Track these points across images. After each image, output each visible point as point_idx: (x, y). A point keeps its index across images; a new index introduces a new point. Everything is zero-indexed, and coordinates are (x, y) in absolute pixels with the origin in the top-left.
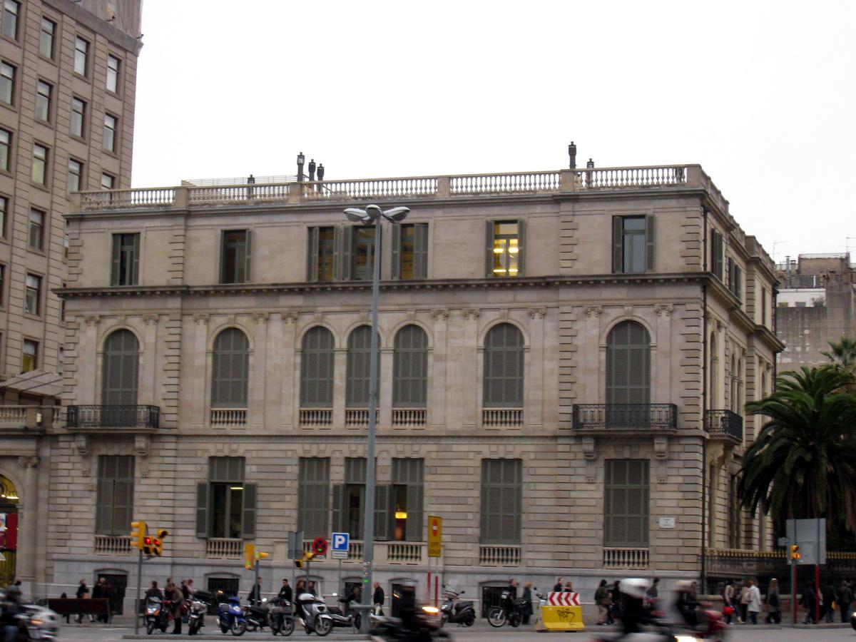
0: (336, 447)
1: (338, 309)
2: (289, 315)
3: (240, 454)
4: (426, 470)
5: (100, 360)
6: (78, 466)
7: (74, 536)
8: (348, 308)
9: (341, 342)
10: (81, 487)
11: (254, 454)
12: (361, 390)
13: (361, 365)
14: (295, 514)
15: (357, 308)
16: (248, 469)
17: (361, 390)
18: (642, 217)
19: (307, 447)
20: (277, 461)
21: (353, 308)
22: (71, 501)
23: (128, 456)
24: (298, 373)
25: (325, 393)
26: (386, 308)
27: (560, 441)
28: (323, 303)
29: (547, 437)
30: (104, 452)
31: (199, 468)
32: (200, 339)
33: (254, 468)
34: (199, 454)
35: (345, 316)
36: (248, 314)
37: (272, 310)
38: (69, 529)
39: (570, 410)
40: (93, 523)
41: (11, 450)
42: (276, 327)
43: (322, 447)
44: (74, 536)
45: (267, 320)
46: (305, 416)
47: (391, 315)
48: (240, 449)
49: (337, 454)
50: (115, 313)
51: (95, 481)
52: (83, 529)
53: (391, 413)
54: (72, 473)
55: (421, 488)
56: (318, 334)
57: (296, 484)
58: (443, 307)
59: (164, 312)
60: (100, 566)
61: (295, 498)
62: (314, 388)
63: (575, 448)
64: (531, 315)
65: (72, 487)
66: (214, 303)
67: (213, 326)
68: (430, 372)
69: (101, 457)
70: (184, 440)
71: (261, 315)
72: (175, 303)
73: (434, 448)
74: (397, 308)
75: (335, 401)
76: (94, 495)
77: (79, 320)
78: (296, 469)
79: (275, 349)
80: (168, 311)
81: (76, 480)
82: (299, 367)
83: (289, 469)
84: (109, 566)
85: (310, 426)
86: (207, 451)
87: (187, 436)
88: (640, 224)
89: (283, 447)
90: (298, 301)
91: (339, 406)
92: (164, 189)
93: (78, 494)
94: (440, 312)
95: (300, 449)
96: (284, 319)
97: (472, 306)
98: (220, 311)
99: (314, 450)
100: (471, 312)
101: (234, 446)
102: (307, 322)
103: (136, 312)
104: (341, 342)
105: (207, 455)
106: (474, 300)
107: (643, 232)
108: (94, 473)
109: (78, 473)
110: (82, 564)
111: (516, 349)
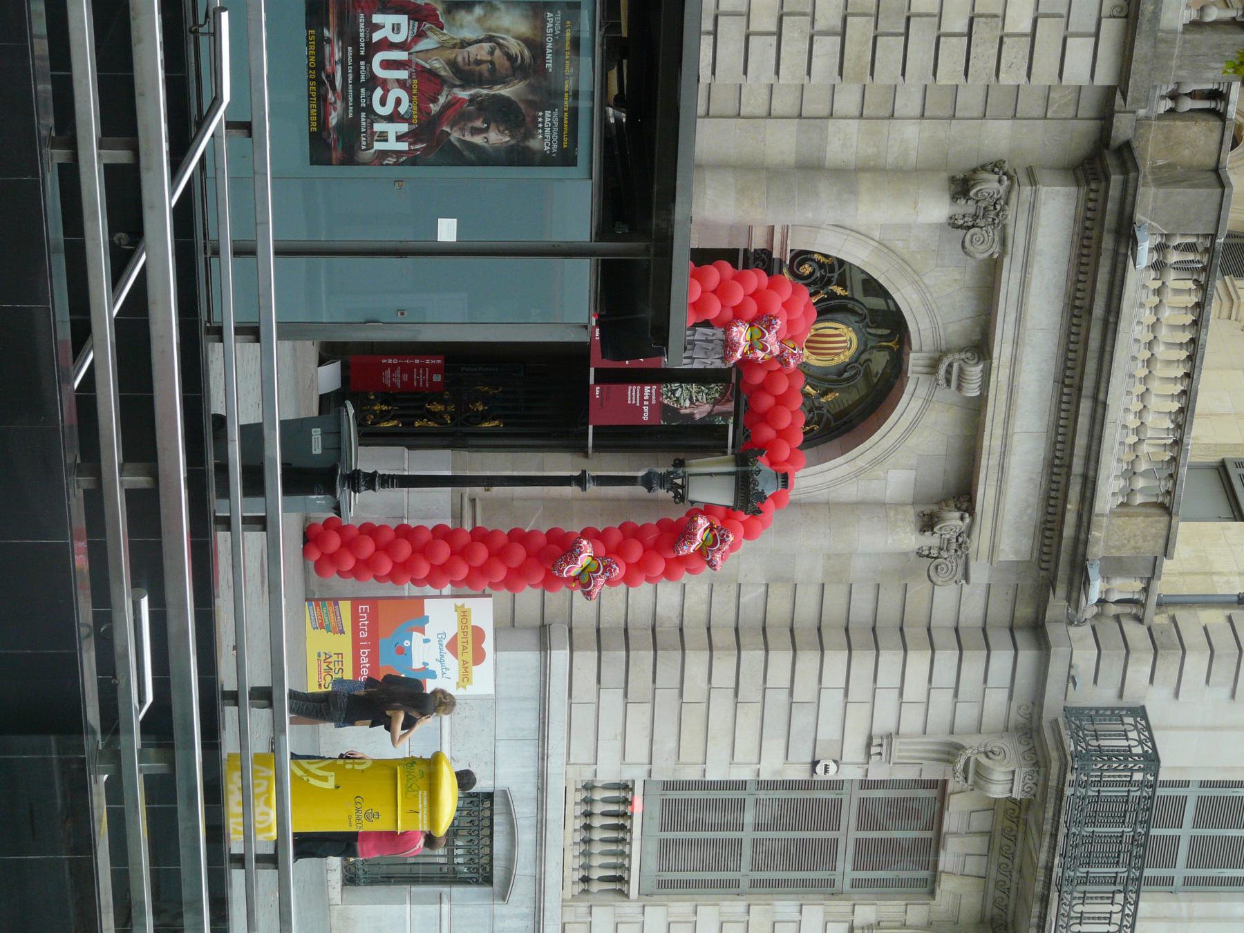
6: (912, 721)
7: (639, 715)
10: (828, 732)
22: (777, 699)
38: (666, 698)
40: (692, 774)
41: (1002, 468)
44: (639, 715)
51: (851, 773)
52: (666, 743)
54: (886, 701)
60: (524, 812)
65: (832, 700)
84: (526, 837)
93: (802, 719)
110: (531, 750)
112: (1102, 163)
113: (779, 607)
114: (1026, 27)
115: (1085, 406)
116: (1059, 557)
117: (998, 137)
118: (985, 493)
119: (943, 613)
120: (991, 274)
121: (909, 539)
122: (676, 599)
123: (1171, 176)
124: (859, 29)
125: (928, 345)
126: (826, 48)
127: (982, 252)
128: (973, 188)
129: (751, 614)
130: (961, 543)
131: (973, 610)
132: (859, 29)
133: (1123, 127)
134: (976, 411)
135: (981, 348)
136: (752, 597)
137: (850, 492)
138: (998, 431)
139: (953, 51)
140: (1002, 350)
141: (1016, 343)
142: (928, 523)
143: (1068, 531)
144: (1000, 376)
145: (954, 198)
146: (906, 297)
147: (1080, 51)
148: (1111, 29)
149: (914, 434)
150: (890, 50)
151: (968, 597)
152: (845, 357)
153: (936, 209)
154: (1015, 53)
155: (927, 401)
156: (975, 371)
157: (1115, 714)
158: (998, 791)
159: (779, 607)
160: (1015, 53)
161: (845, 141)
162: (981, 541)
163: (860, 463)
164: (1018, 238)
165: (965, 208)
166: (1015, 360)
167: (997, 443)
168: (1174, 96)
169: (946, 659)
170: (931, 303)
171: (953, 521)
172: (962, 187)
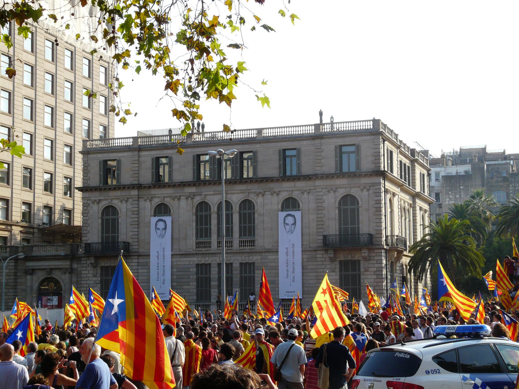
0: (213, 258)
1: (212, 193)
2: (189, 196)
4: (256, 268)
5: (100, 221)
8: (217, 192)
14: (195, 291)
18: (295, 149)
19: (200, 259)
21: (219, 192)
24: (194, 224)
25: (207, 233)
26: (235, 192)
27: (318, 252)
29: (312, 251)
30: (103, 265)
35: (215, 196)
36: (170, 197)
37: (181, 194)
39: (322, 237)
42: (183, 202)
43: (207, 259)
45: (179, 199)
46: (198, 244)
47: (237, 195)
49: (214, 262)
50: (106, 198)
51: (99, 279)
53: (238, 242)
54: (88, 275)
55: (210, 278)
57: (195, 277)
58: (261, 191)
59: (130, 197)
61: (195, 283)
63: (325, 256)
64: (258, 195)
65: (88, 282)
66: (154, 192)
67: (153, 202)
68: (256, 221)
69: (102, 268)
70: (141, 257)
71: (176, 197)
72: (135, 192)
73: (259, 257)
75: (212, 237)
76: (99, 285)
77: (89, 202)
78: (195, 270)
80: (132, 197)
81: (90, 279)
83: (191, 270)
85: (201, 249)
87: (143, 256)
88: (294, 153)
89: (189, 259)
90: (193, 190)
91: (214, 239)
92: (128, 138)
94: (260, 193)
95: (196, 260)
96: (187, 198)
97: (275, 190)
98: (157, 196)
99: (203, 260)
100: (275, 192)
102: (198, 199)
103: (116, 197)
107: (295, 156)
108: (98, 275)
109: (91, 275)
111: (208, 213)
144: (47, 267)
146: (42, 278)
149: (56, 275)
170: (41, 276)
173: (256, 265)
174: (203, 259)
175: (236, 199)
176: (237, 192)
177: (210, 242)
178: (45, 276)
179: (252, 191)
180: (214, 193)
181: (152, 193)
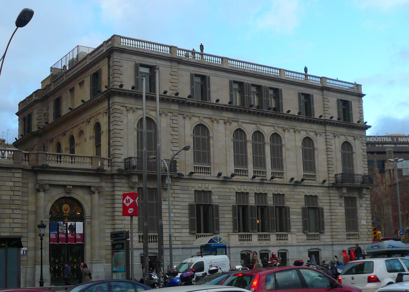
1: (248, 121)
3: (210, 189)
4: (285, 199)
8: (252, 122)
9: (249, 137)
11: (216, 190)
12: (259, 161)
13: (259, 150)
15: (256, 122)
16: (213, 197)
17: (259, 161)
20: (226, 194)
21: (254, 122)
23: (154, 188)
28: (242, 118)
31: (190, 196)
32: (187, 128)
33: (217, 197)
34: (190, 188)
37: (220, 118)
41: (84, 182)
42: (221, 127)
47: (268, 127)
48: (210, 187)
49: (252, 191)
56: (239, 133)
58: (287, 127)
62: (240, 159)
68: (284, 155)
72: (175, 107)
74: (270, 124)
77: (122, 108)
79: (221, 137)
82: (211, 146)
83: (232, 198)
86: (193, 187)
91: (250, 168)
94: (287, 129)
96: (225, 123)
97: (297, 128)
98: (196, 115)
100: (298, 130)
101: (207, 185)
104: (249, 137)
105: (193, 189)
106: (298, 125)
112: (36, 171)
113: (110, 214)
114: (13, 183)
115: (73, 171)
116: (99, 173)
117: (31, 185)
118: (88, 184)
119: (110, 189)
120: (51, 185)
121: (96, 196)
122: (108, 230)
123: (37, 160)
124: (13, 207)
125: (65, 194)
126: (15, 212)
127: (48, 187)
128: (40, 188)
129: (110, 218)
130: (97, 188)
131: (110, 185)
132: (13, 207)
133: (29, 168)
134: (74, 187)
135: (64, 186)
136: (107, 218)
137: (89, 204)
138: (78, 183)
139: (16, 193)
140: (65, 183)
141: (64, 181)
142: (94, 193)
143: (94, 172)
144: (69, 183)
145: (40, 192)
146: (57, 198)
147: (17, 175)
148: (13, 171)
149: (79, 195)
150: (15, 202)
151: (106, 186)
152: (68, 206)
153: (42, 194)
154: (17, 184)
155: (73, 193)
156: (68, 187)
157: (125, 163)
158: (137, 180)
159: (110, 214)
160: (17, 184)
161: (32, 208)
162: (97, 185)
163: (84, 203)
164: (47, 182)
165: (41, 190)
166: (66, 181)
167: (80, 183)
168: (25, 160)
169: (116, 189)
170: (57, 194)
171: (92, 189)
172: (38, 191)
173: (286, 196)
174: (242, 187)
175: (267, 132)
176: (269, 124)
177: (283, 173)
178: (62, 195)
179: (280, 126)
180: (250, 122)
181: (191, 111)
